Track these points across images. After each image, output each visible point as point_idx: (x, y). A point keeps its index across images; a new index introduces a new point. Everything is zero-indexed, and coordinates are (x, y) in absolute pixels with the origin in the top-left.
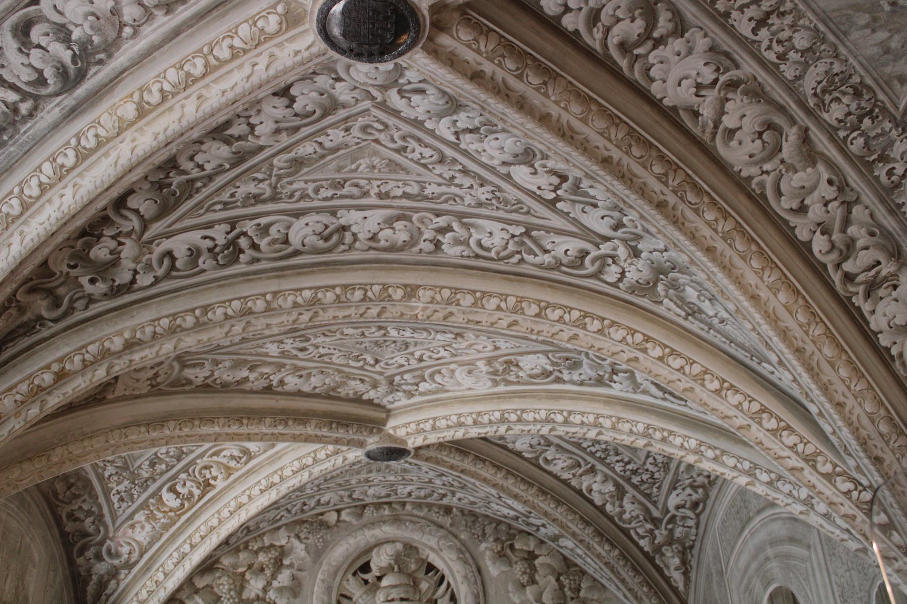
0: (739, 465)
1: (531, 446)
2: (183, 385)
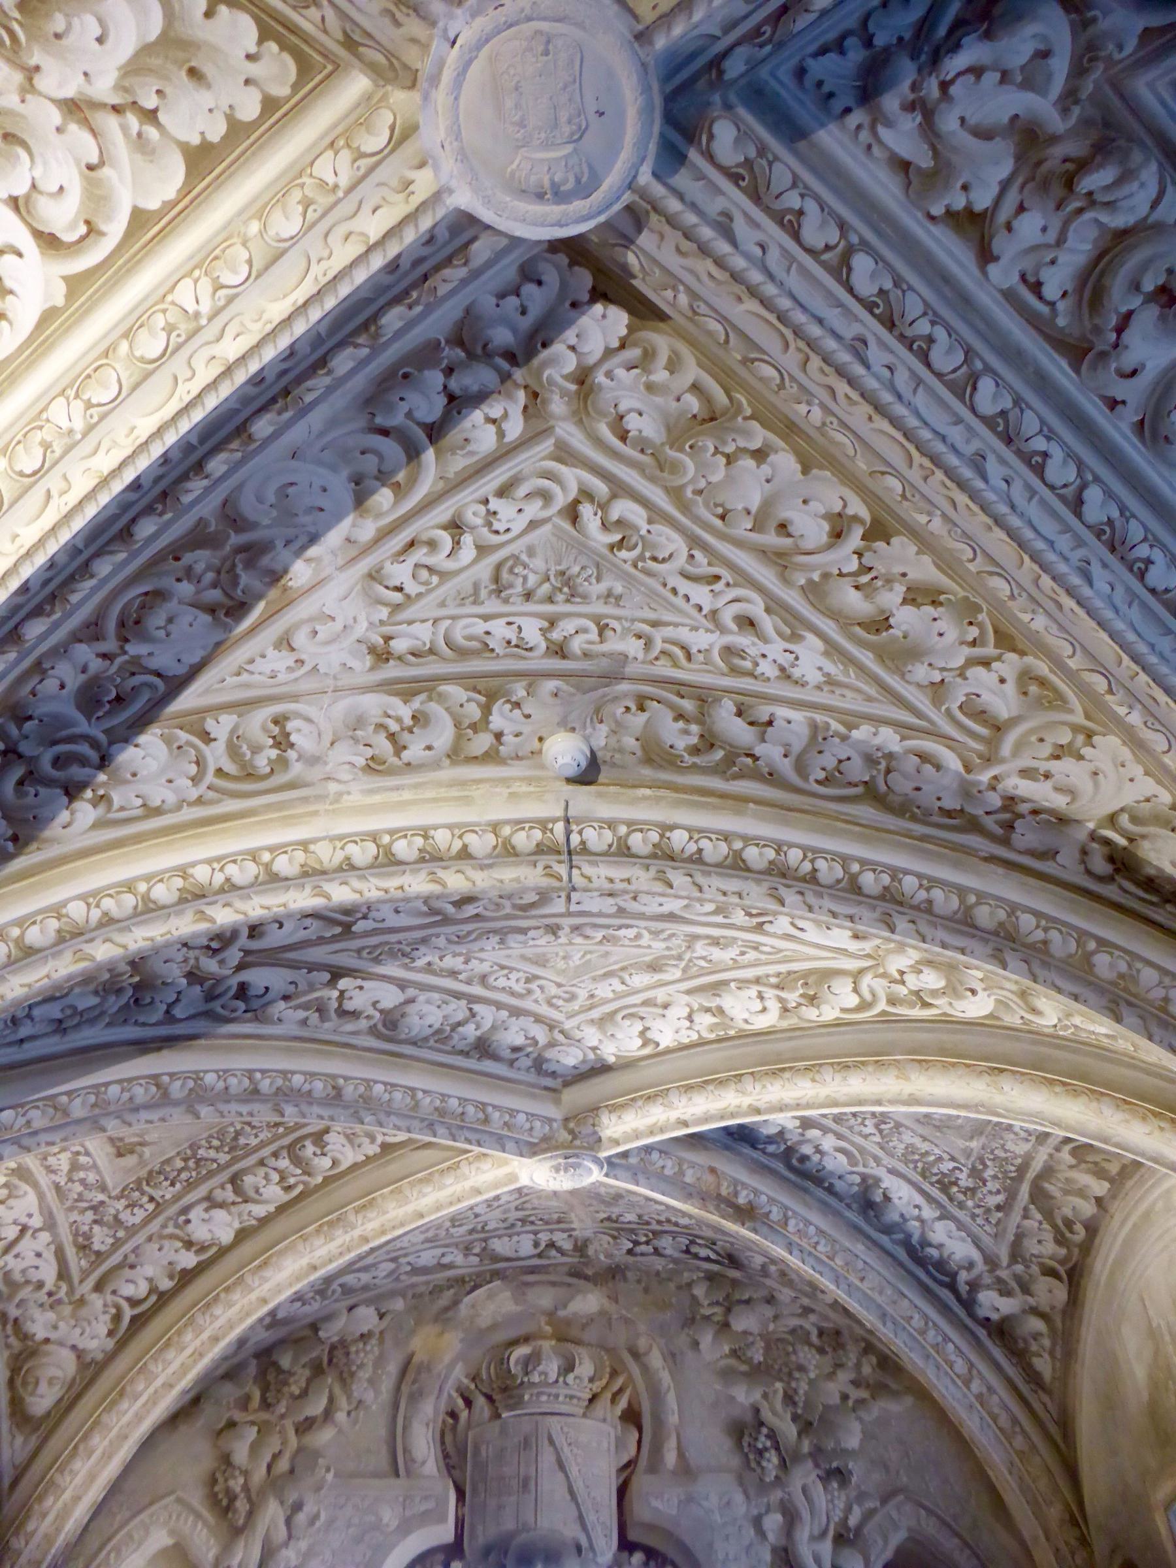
2: (1042, 682)
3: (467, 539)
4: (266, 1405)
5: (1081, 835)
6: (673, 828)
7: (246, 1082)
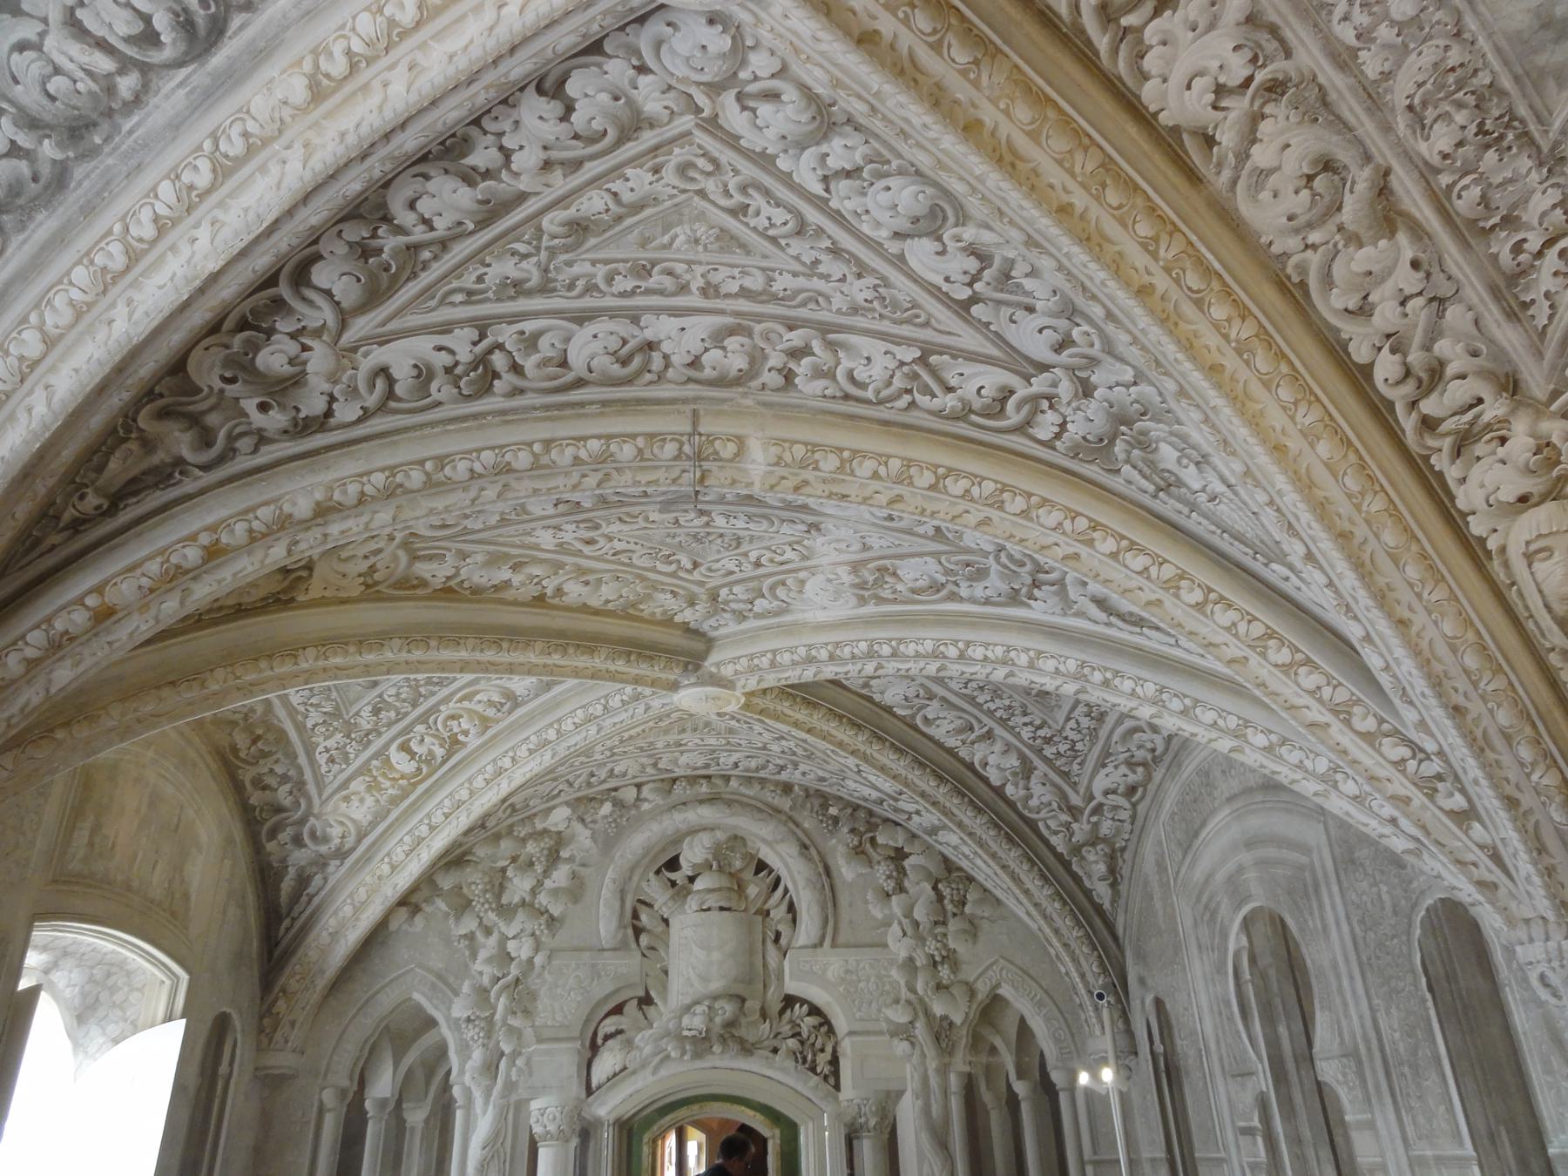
0: (1221, 722)
1: (906, 699)
2: (414, 587)
3: (753, 559)
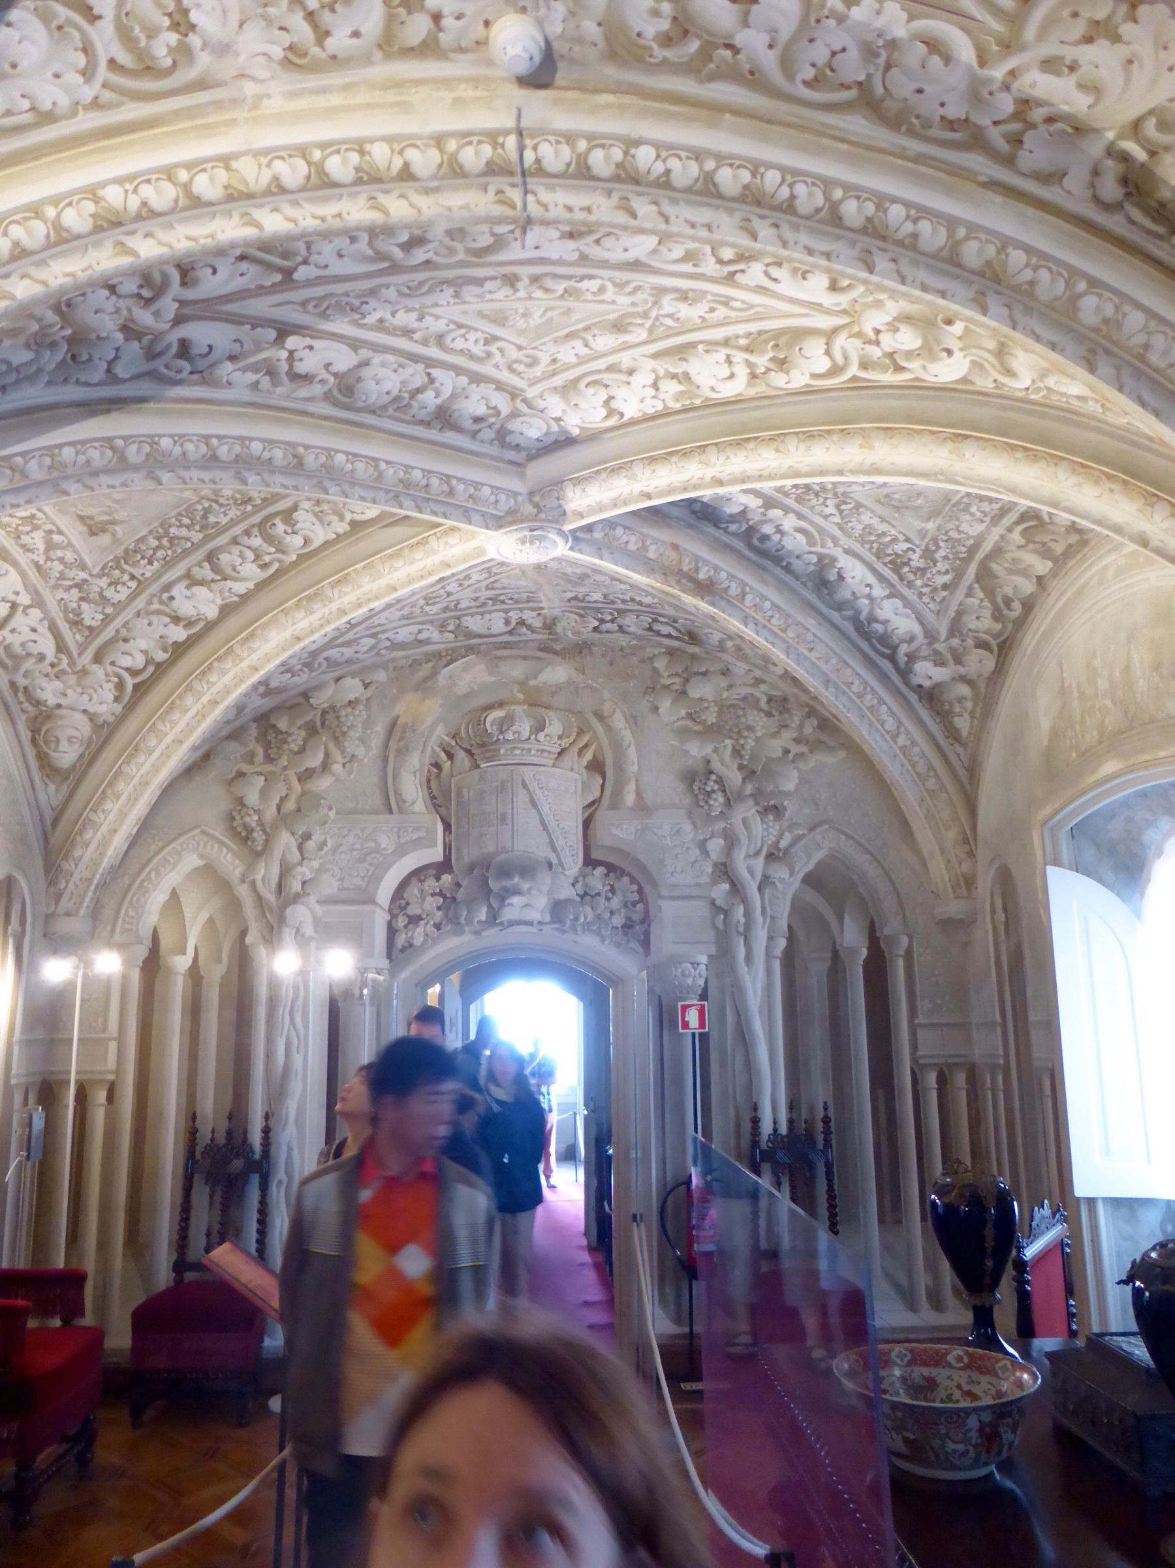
4: (269, 759)
5: (1095, 149)
6: (638, 143)
7: (204, 449)
